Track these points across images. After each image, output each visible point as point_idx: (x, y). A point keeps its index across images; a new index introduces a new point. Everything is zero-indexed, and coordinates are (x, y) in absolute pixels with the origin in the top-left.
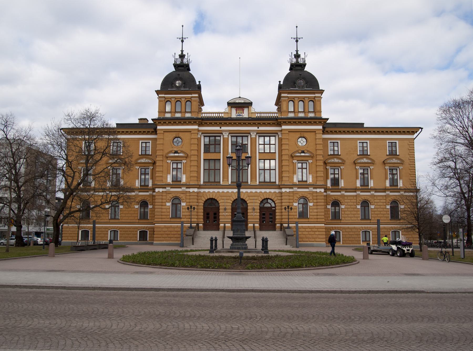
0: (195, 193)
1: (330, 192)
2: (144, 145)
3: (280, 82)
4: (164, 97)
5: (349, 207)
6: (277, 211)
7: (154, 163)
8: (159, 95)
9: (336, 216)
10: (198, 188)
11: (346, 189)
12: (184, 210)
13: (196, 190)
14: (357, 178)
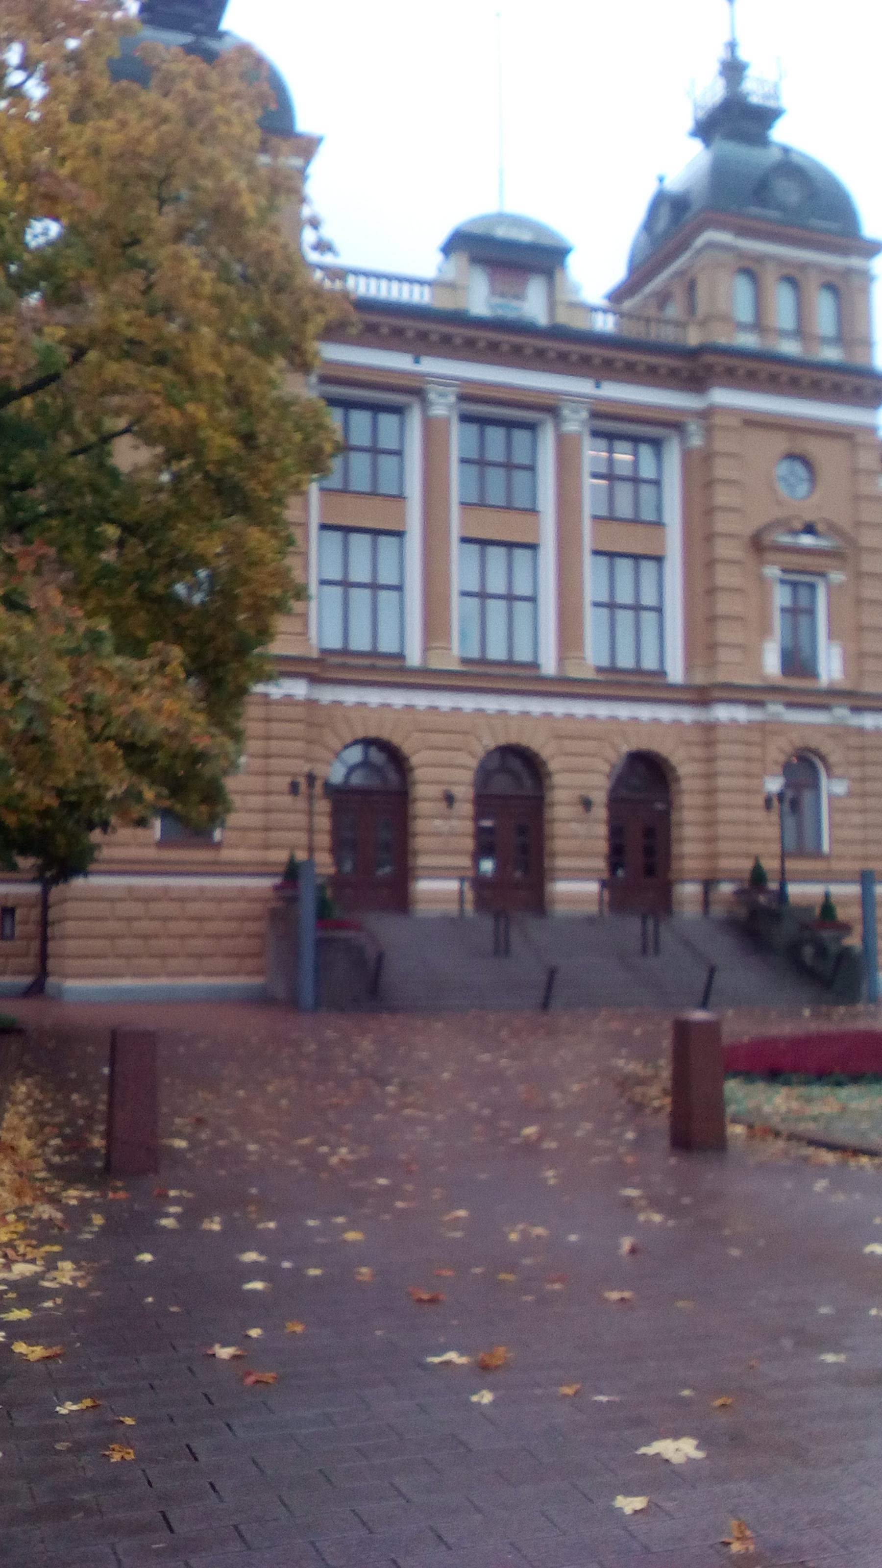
0: (298, 704)
10: (314, 680)
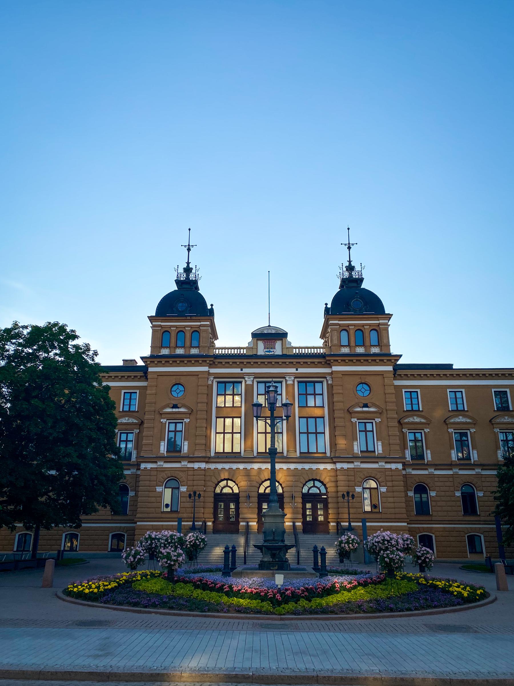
0: (202, 470)
1: (410, 470)
2: (128, 396)
3: (326, 304)
4: (160, 326)
5: (443, 494)
6: (330, 500)
7: (142, 423)
8: (154, 323)
9: (423, 509)
10: (207, 462)
11: (436, 465)
12: (184, 499)
13: (203, 465)
14: (452, 448)
